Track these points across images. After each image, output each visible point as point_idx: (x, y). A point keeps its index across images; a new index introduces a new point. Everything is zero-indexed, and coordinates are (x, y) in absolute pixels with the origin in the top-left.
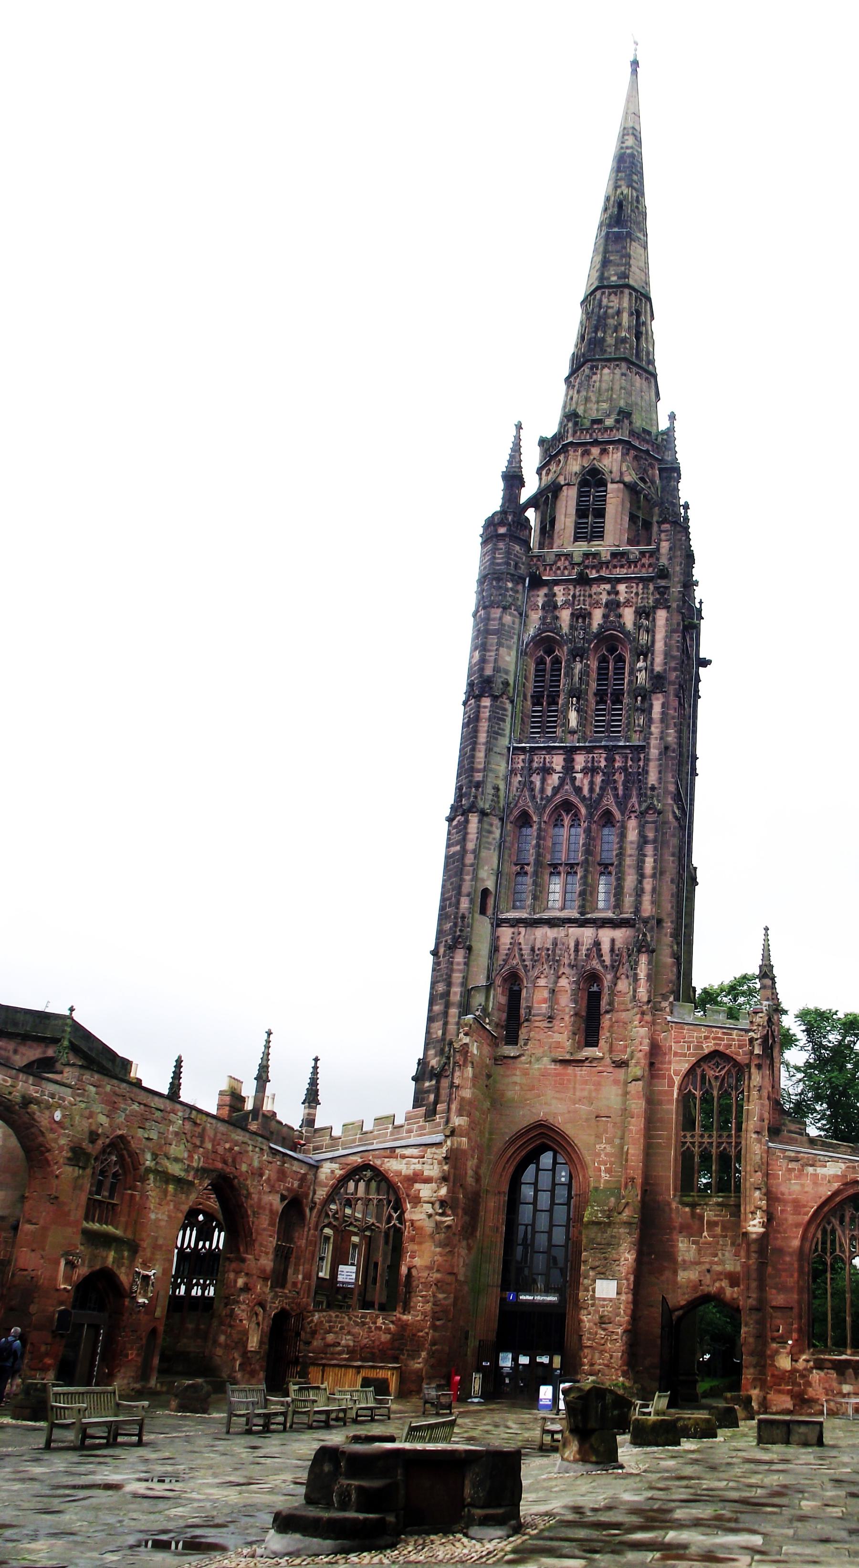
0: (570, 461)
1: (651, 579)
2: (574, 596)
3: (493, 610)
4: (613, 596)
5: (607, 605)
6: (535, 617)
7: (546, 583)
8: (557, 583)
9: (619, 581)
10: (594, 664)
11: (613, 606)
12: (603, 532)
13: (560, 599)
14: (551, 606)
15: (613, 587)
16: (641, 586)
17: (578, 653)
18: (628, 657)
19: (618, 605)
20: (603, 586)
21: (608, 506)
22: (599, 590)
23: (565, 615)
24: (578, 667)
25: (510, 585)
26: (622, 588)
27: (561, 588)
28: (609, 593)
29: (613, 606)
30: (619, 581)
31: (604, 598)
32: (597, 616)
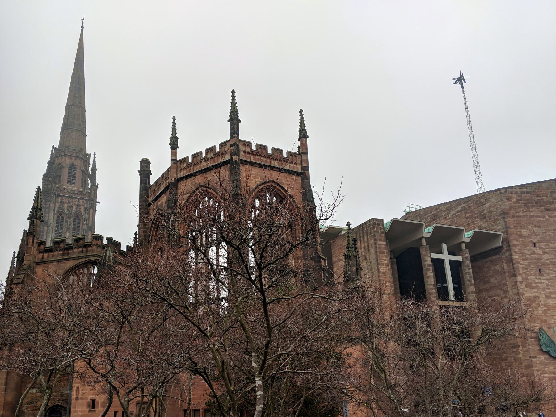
0: (67, 159)
1: (89, 200)
2: (68, 201)
3: (48, 202)
4: (79, 203)
5: (77, 205)
6: (57, 205)
7: (61, 196)
8: (64, 196)
9: (81, 199)
10: (72, 220)
11: (78, 206)
12: (75, 182)
13: (64, 201)
14: (62, 202)
15: (79, 201)
16: (86, 201)
17: (69, 217)
18: (82, 220)
19: (80, 206)
20: (76, 200)
21: (77, 173)
22: (75, 200)
23: (66, 205)
24: (69, 221)
25: (52, 195)
26: (81, 201)
27: (65, 198)
28: (78, 202)
29: (78, 206)
30: (81, 199)
31: (76, 203)
32: (74, 207)
